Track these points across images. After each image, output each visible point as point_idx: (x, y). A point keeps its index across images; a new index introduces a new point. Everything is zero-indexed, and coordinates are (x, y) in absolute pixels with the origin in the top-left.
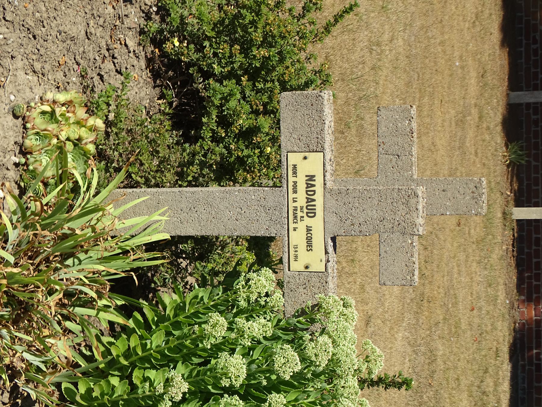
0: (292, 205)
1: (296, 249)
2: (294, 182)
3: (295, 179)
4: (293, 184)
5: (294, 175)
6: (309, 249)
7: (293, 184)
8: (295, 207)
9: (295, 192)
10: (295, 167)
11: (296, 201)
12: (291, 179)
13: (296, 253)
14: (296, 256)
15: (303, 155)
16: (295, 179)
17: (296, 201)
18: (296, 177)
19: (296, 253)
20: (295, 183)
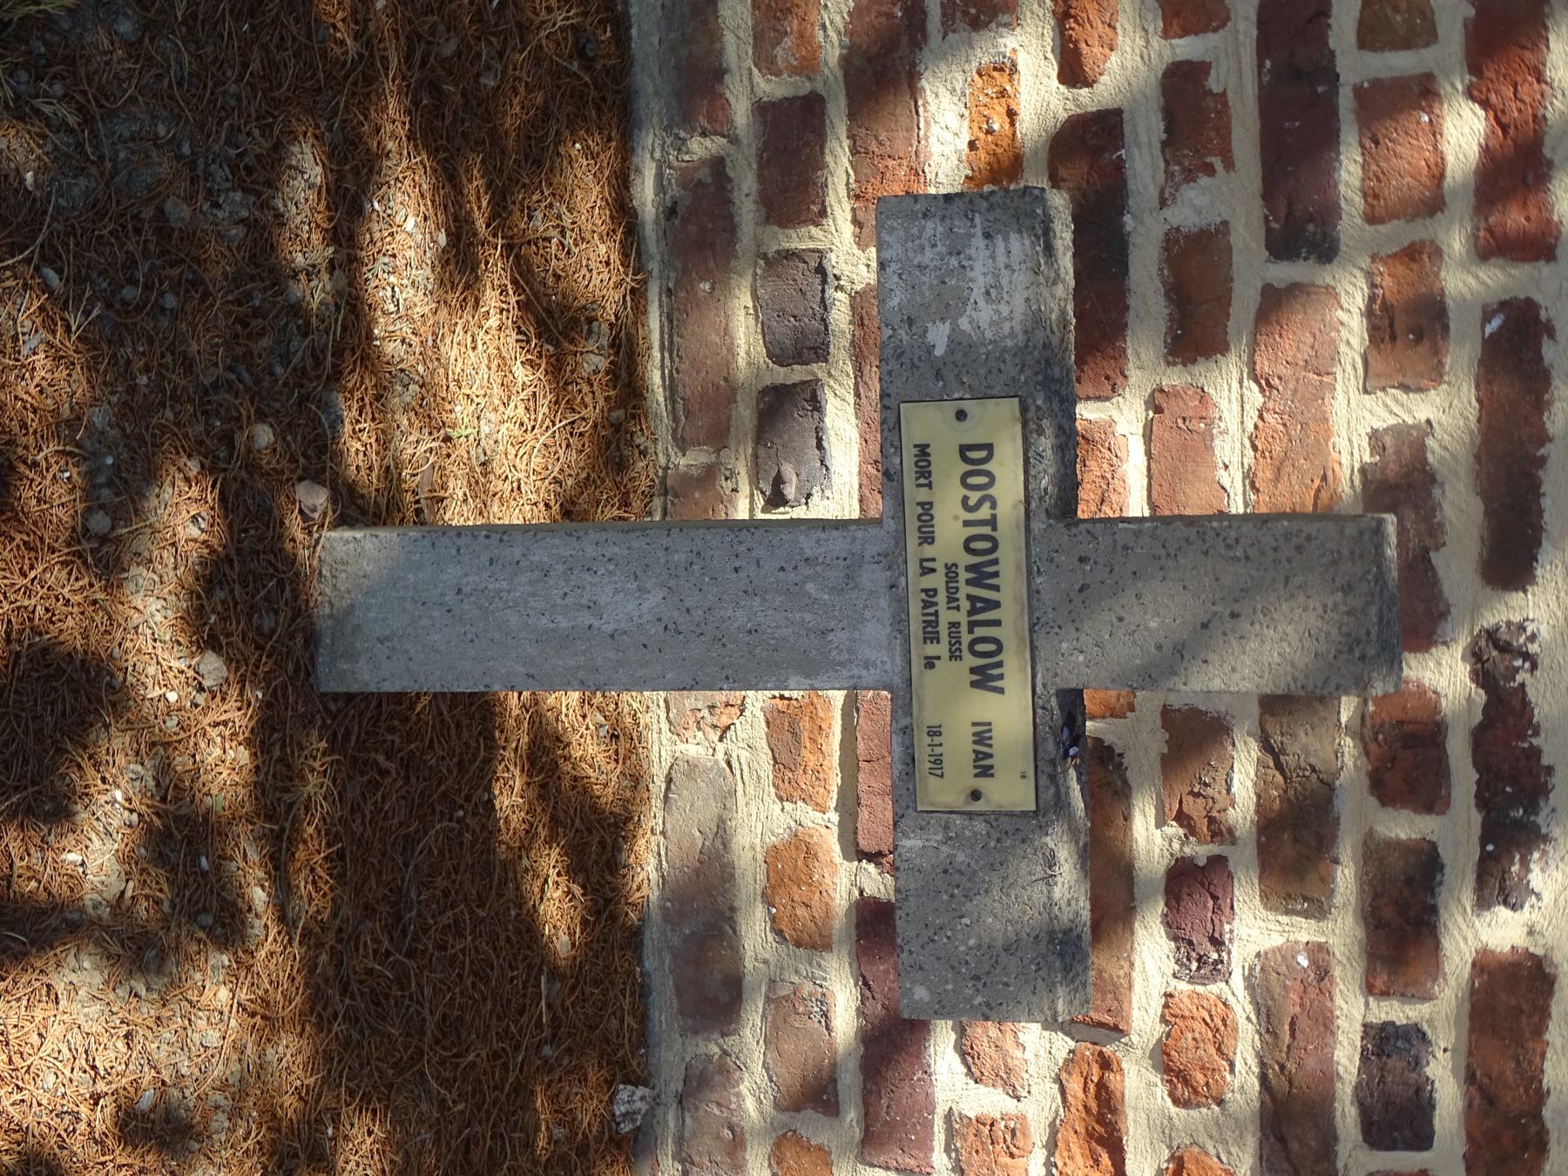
0: (916, 583)
1: (937, 740)
2: (921, 504)
3: (923, 495)
4: (920, 511)
5: (922, 481)
6: (974, 497)
7: (920, 511)
8: (925, 591)
9: (927, 538)
10: (923, 451)
11: (933, 570)
12: (914, 494)
13: (938, 750)
14: (938, 761)
15: (950, 408)
16: (923, 495)
17: (933, 570)
18: (930, 486)
19: (938, 750)
20: (927, 506)
